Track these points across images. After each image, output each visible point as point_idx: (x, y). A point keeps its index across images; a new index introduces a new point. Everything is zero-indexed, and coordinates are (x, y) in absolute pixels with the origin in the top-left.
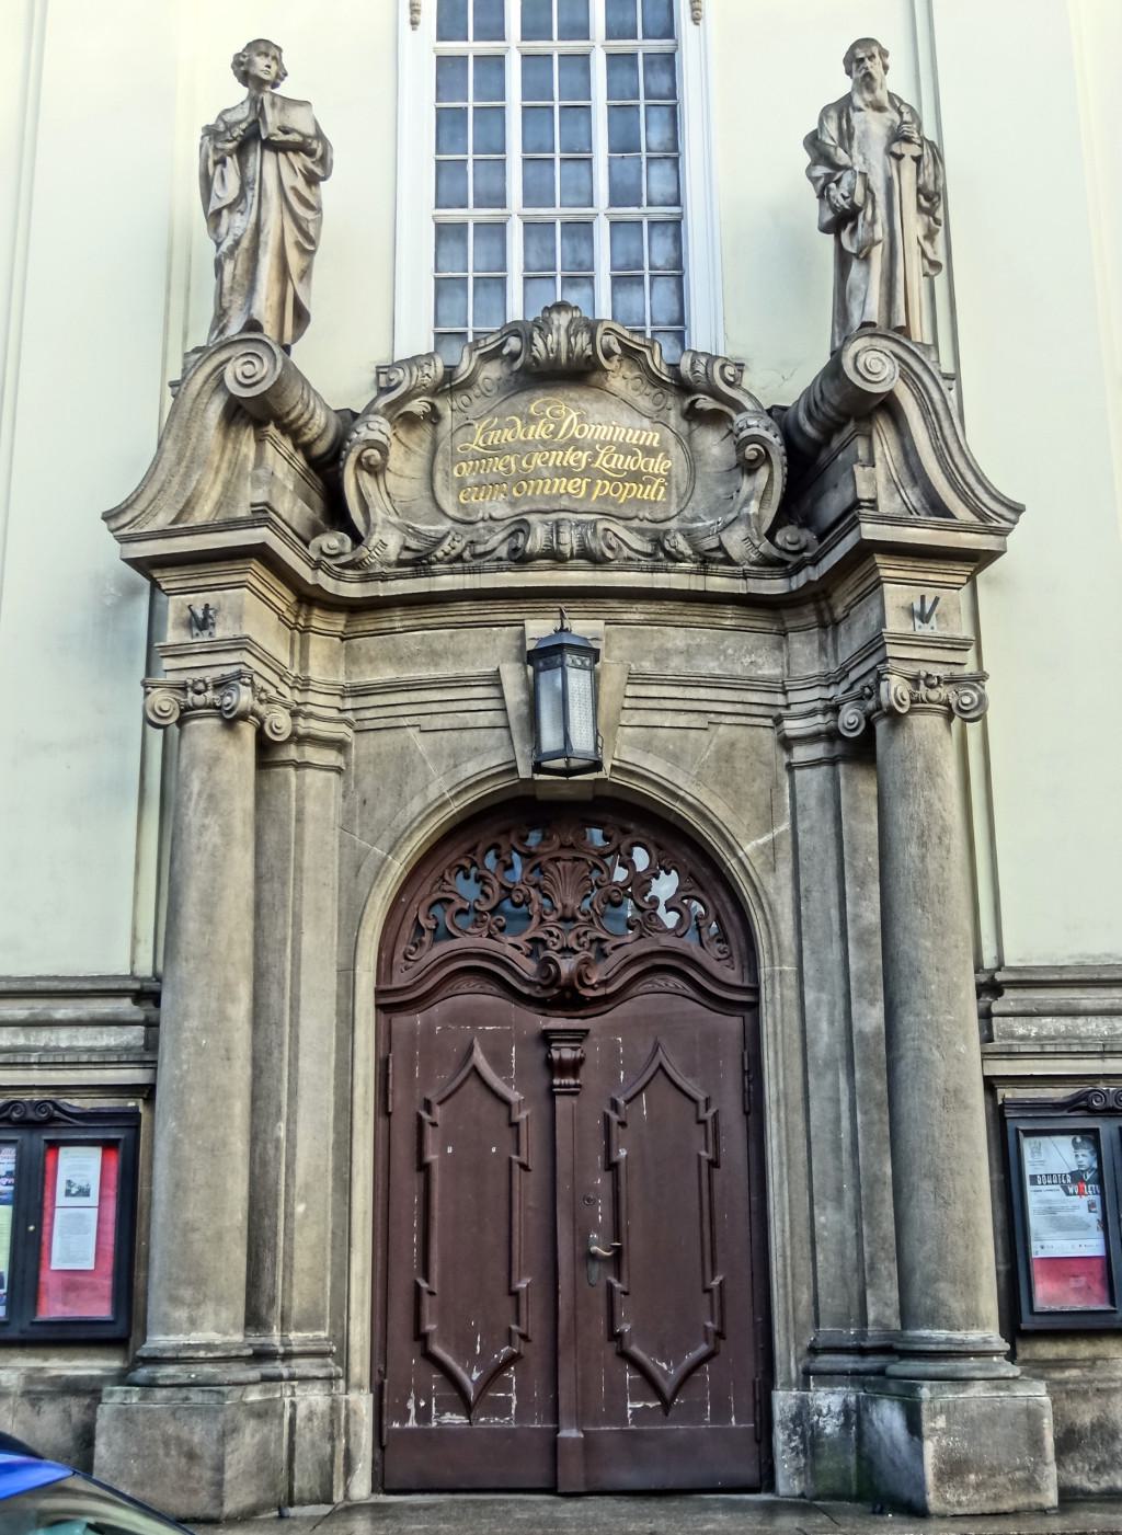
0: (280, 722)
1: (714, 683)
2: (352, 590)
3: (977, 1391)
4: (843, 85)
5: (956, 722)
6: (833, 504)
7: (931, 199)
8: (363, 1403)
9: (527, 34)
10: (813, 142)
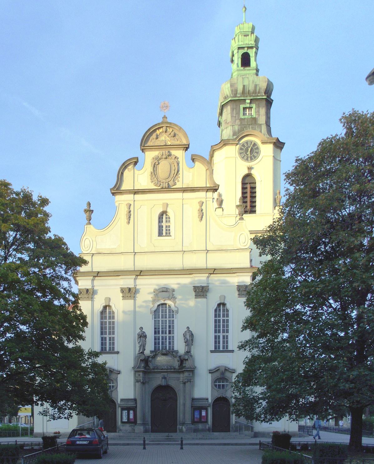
0: (144, 381)
1: (175, 378)
2: (149, 371)
3: (189, 426)
4: (186, 330)
5: (191, 382)
6: (184, 365)
7: (192, 340)
8: (150, 427)
9: (162, 318)
10: (184, 334)
